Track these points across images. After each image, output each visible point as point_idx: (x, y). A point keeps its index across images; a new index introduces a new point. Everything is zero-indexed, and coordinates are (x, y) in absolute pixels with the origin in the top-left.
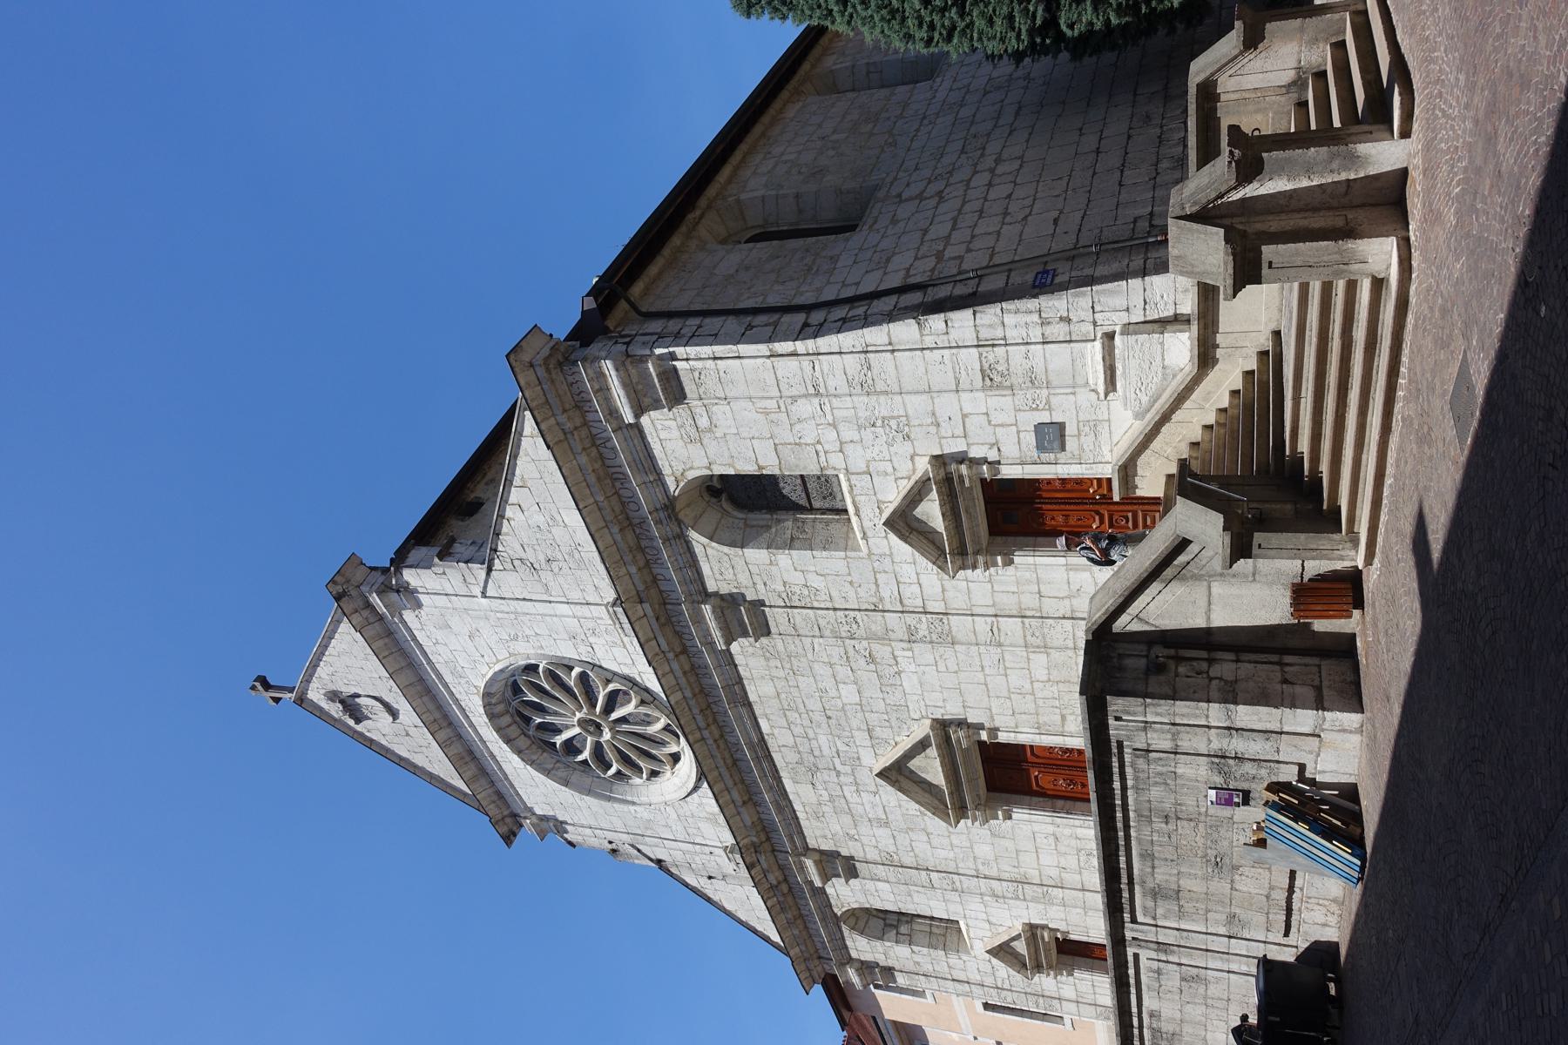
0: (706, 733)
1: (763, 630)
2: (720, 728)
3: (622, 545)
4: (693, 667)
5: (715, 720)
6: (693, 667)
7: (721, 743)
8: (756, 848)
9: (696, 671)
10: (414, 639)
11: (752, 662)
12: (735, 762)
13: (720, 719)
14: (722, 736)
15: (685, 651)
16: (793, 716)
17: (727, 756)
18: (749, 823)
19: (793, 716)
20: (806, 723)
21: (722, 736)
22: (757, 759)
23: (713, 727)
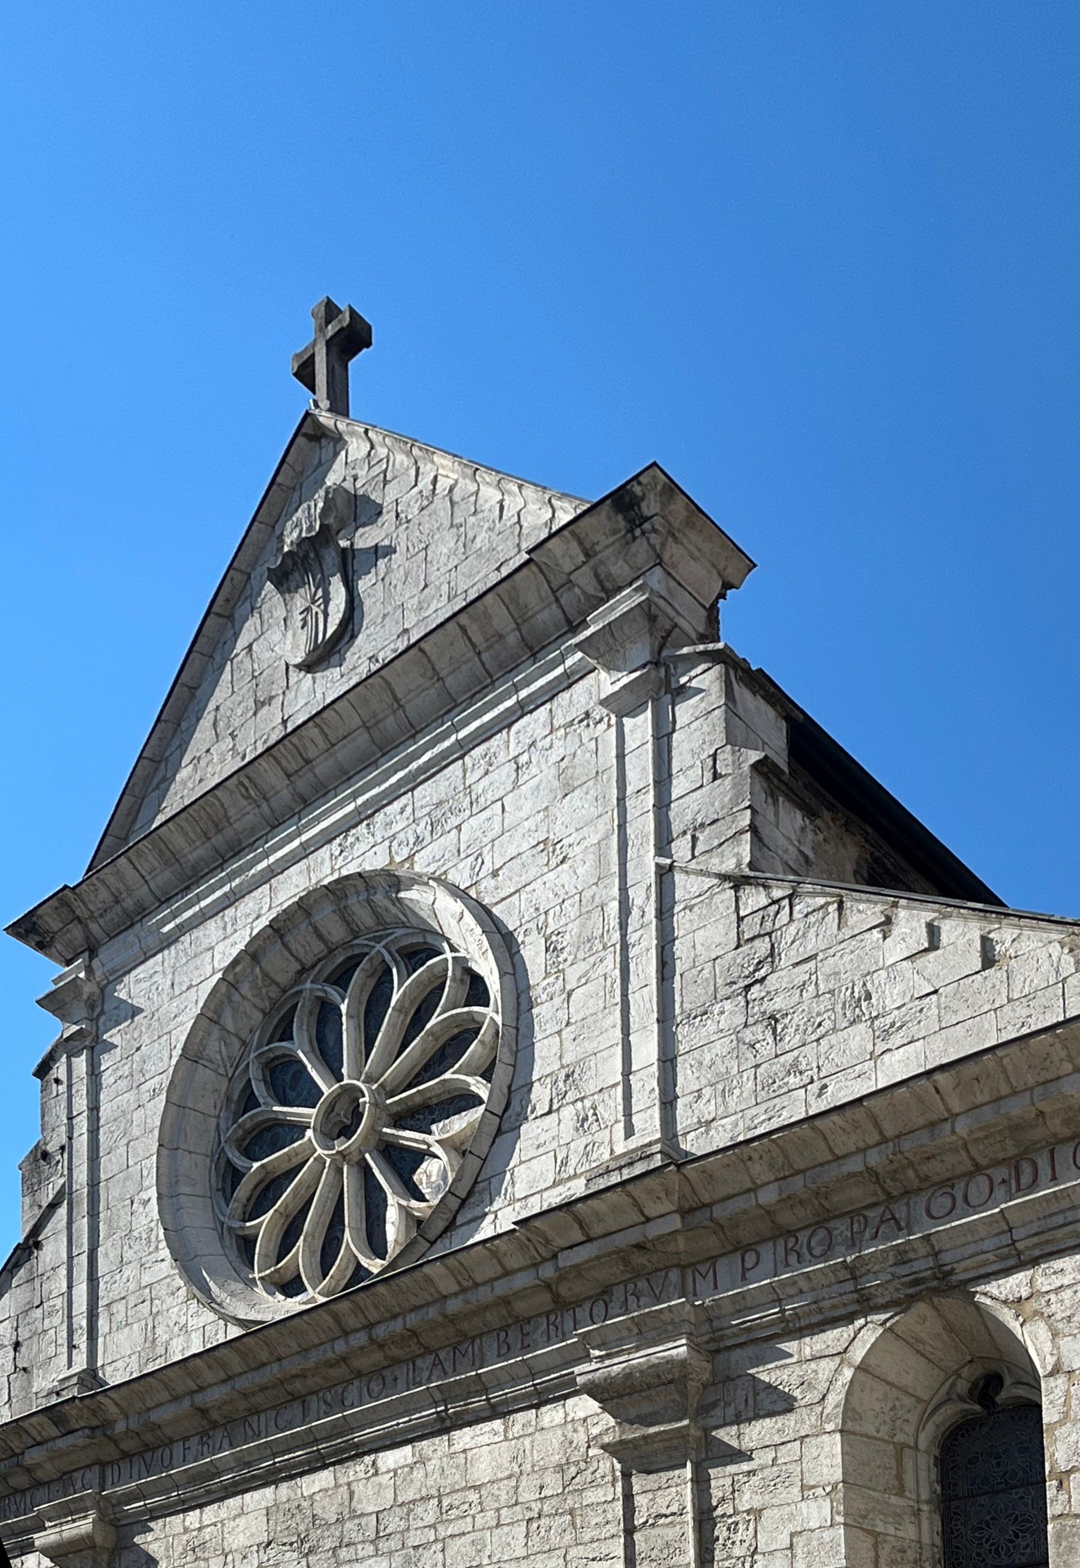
0: (360, 1339)
1: (636, 1459)
2: (379, 1372)
3: (834, 1172)
4: (522, 1322)
5: (395, 1362)
6: (522, 1322)
7: (341, 1371)
8: (101, 1428)
9: (513, 1326)
10: (523, 709)
11: (555, 1439)
12: (302, 1399)
13: (401, 1372)
14: (359, 1375)
15: (561, 1305)
16: (428, 1513)
17: (311, 1382)
18: (154, 1416)
19: (428, 1513)
20: (414, 1539)
21: (359, 1375)
22: (310, 1439)
23: (377, 1357)
